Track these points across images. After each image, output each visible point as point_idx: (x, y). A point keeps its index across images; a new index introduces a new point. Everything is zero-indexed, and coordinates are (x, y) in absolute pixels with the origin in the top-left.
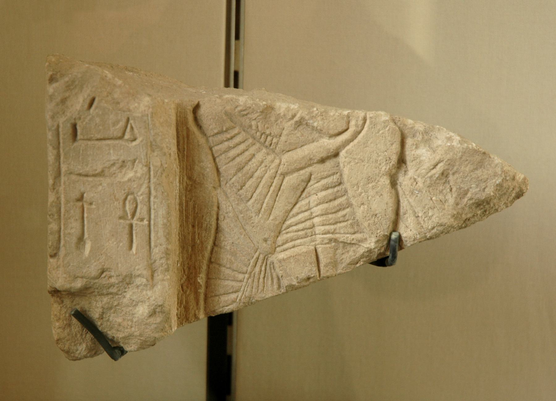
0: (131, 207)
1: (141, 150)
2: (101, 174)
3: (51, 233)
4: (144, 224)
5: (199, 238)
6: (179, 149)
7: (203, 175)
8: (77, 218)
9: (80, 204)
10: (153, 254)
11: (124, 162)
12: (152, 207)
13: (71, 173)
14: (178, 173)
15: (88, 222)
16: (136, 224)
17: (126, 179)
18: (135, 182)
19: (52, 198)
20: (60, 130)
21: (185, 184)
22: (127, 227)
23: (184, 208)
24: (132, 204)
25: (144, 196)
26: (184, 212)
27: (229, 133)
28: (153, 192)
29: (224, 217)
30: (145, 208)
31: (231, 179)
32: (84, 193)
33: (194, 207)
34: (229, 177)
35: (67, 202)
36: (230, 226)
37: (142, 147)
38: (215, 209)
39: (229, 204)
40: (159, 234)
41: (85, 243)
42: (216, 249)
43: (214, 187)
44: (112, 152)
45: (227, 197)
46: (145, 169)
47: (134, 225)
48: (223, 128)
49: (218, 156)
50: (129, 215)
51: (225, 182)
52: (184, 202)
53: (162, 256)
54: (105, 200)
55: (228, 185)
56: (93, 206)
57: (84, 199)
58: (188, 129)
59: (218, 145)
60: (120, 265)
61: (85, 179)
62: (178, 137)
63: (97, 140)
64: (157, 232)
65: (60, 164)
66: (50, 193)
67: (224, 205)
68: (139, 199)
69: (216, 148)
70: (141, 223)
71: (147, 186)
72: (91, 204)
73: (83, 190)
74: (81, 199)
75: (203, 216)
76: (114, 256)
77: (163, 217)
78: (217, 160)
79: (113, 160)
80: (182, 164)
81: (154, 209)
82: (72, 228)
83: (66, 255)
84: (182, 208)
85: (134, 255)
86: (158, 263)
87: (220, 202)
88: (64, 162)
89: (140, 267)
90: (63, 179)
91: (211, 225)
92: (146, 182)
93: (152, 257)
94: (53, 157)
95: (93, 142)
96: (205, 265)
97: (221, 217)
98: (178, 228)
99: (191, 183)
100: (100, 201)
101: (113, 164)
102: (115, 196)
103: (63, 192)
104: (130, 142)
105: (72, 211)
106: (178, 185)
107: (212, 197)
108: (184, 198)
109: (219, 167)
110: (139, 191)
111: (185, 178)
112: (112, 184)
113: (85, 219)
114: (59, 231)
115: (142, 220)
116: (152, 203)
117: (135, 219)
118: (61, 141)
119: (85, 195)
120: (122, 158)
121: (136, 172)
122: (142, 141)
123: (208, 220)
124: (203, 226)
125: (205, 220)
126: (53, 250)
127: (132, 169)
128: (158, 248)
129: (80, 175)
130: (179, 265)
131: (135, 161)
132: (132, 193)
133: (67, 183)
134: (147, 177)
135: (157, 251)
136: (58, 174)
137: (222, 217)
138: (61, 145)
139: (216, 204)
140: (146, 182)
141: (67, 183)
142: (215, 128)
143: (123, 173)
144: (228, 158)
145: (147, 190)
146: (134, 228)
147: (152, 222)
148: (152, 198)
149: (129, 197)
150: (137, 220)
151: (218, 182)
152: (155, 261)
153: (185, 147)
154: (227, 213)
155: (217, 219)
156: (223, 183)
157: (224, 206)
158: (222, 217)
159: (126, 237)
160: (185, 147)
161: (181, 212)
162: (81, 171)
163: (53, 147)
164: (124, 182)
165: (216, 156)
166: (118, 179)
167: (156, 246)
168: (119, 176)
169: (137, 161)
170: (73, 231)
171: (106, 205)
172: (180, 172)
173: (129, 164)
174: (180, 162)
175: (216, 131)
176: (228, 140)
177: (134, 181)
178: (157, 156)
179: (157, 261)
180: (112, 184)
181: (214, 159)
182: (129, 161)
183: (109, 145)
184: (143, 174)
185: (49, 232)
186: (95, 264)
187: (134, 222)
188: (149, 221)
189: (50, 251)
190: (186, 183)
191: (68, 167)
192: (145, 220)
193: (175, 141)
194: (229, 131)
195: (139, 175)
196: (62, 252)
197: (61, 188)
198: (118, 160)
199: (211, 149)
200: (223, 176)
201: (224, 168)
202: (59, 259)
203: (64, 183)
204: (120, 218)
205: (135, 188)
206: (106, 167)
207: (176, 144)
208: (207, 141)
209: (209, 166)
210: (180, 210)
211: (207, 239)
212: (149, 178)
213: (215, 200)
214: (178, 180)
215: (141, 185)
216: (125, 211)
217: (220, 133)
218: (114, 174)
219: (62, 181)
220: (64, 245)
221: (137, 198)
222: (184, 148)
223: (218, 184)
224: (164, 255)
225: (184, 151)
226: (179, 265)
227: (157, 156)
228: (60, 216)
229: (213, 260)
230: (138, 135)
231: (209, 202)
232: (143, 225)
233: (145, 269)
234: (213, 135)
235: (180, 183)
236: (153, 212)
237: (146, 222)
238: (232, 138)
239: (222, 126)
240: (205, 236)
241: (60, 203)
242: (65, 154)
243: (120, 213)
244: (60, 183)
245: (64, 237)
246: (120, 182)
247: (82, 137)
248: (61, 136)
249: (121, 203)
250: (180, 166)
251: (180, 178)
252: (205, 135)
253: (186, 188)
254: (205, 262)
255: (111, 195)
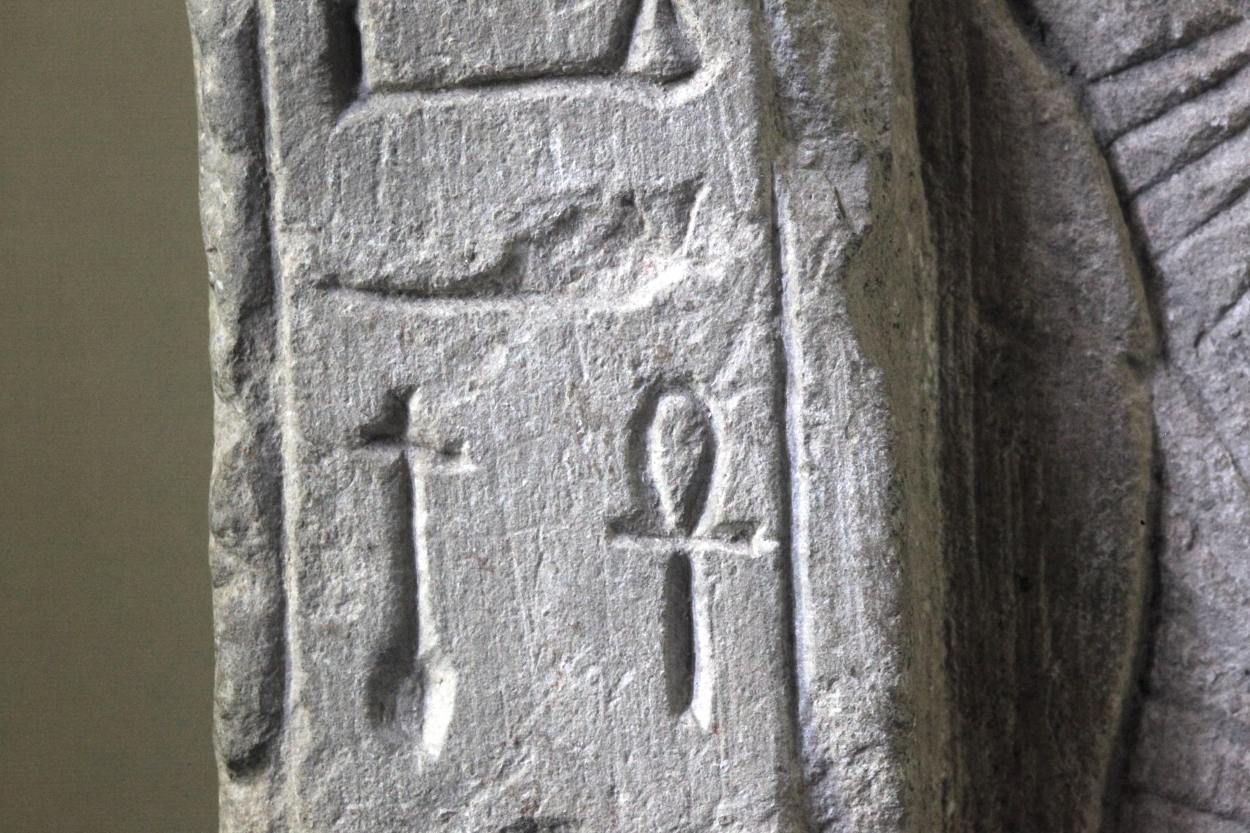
0: (679, 464)
1: (727, 130)
2: (503, 278)
3: (234, 635)
4: (755, 554)
5: (1057, 652)
6: (927, 150)
7: (1071, 290)
8: (373, 536)
9: (390, 456)
10: (807, 733)
11: (626, 200)
12: (799, 456)
13: (331, 283)
14: (932, 286)
15: (438, 553)
16: (708, 557)
17: (641, 300)
18: (699, 316)
19: (230, 428)
20: (267, 38)
21: (971, 347)
22: (659, 575)
23: (970, 481)
24: (684, 442)
25: (750, 391)
26: (972, 505)
27: (1204, 54)
28: (800, 368)
29: (1195, 531)
30: (759, 463)
31: (1224, 311)
32: (410, 391)
33: (1026, 478)
34: (1216, 301)
35: (316, 451)
36: (1228, 579)
37: (731, 110)
38: (1144, 481)
39: (1216, 451)
40: (844, 611)
41: (422, 681)
42: (1153, 712)
43: (1132, 361)
44: (557, 145)
45: (1208, 419)
46: (751, 237)
47: (698, 567)
48: (1166, 28)
49: (1141, 191)
50: (667, 505)
51: (1190, 331)
52: (969, 446)
53: (863, 737)
54: (530, 424)
55: (1208, 347)
56: (464, 466)
57: (413, 432)
58: (975, 34)
59: (1146, 121)
60: (623, 799)
61: (411, 309)
62: (922, 83)
63: (476, 83)
64: (831, 598)
65: (267, 235)
66: (221, 410)
67: (1191, 457)
68: (721, 412)
69: (1136, 139)
70: (740, 550)
71: (761, 332)
72: (449, 452)
73: (398, 374)
74: (389, 425)
75: (1077, 526)
76: (591, 749)
77: (861, 511)
78: (1144, 206)
79: (568, 193)
80: (948, 233)
81: (812, 468)
82: (345, 598)
83: (315, 759)
84: (960, 481)
85: (703, 739)
86: (843, 778)
87: (1166, 445)
88: (290, 220)
89: (740, 803)
90: (288, 317)
91: (1125, 574)
92: (757, 308)
93: (807, 747)
94: (228, 198)
95: (447, 100)
96: (1096, 802)
97: (1178, 531)
98: (941, 597)
99: (1002, 341)
100: (498, 434)
101: (567, 223)
102: (585, 399)
103: (289, 390)
104: (656, 89)
105: (345, 501)
106: (933, 350)
107: (1127, 417)
108: (968, 427)
109: (1156, 246)
110: (719, 365)
111: (972, 312)
112: (567, 333)
113: (421, 544)
114: (276, 619)
115: (740, 530)
116: (796, 433)
117: (702, 527)
118: (272, 102)
119: (415, 404)
120: (617, 181)
121: (699, 257)
122: (724, 77)
123: (1107, 547)
124: (1082, 579)
125: (1091, 548)
126: (246, 732)
127: (677, 241)
128: (837, 695)
129: (381, 288)
130: (952, 806)
131: (685, 194)
132: (682, 383)
133: (312, 342)
134: (764, 281)
135: (835, 711)
136: (258, 301)
137: (1183, 527)
138: (274, 122)
139: (1148, 455)
140: (757, 308)
141: (312, 342)
142: (1125, 29)
143: (625, 268)
144: (1205, 192)
145: (766, 355)
146: (699, 581)
147: (801, 544)
148: (796, 406)
149: (667, 405)
150: (715, 536)
151: (1149, 329)
152: (825, 767)
153: (967, 136)
154: (1208, 505)
155: (1156, 542)
156: (1180, 339)
157: (1194, 468)
158: (1183, 527)
159: (652, 633)
160: (967, 136)
161: (953, 500)
162: (389, 268)
163: (228, 138)
164: (630, 320)
165: (1133, 184)
166: (596, 304)
167: (828, 682)
168: (602, 288)
169: (701, 196)
170: (354, 612)
171: (535, 456)
172: (942, 278)
173: (656, 215)
174: (937, 224)
175: (1129, 45)
176: (1200, 90)
177: (689, 307)
178: (813, 165)
179: (840, 769)
180: (567, 333)
181: (1126, 202)
182: (657, 193)
183: (539, 110)
184: (739, 266)
185: (220, 627)
186: (483, 797)
187: (699, 546)
188: (784, 535)
189: (226, 737)
190: (978, 337)
191: (314, 249)
192: (761, 531)
193: (907, 103)
194: (1202, 45)
195: (715, 271)
196: (298, 737)
197: (283, 372)
198: (593, 191)
199: (1105, 146)
200: (1178, 301)
201: (1184, 247)
202: (278, 780)
203: (297, 343)
204: (616, 527)
205: (694, 349)
206: (526, 239)
207: (913, 121)
208: (1084, 105)
209: (1101, 238)
210: (945, 493)
211: (1104, 652)
212: (776, 290)
213: (1140, 434)
214: (929, 323)
215: (732, 329)
216: (640, 486)
217: (1155, 51)
218: (575, 274)
219: (285, 328)
220: (305, 699)
221: (712, 404)
222: (959, 145)
223: (1151, 344)
224: (875, 731)
225: (960, 159)
226: (952, 806)
227: (813, 165)
228: (275, 531)
229: (1142, 776)
230: (702, 47)
231: (1108, 443)
232: (749, 562)
233: (768, 816)
234: (1116, 71)
235: (942, 343)
236: (801, 482)
237: (762, 545)
238: (1220, 80)
239: (1166, 18)
240: (1091, 640)
241: (276, 460)
242: (298, 175)
243: (613, 498)
244: (273, 344)
245: (306, 652)
246: (611, 321)
247: (387, 74)
248: (272, 73)
249: (620, 441)
250: (940, 245)
251: (941, 313)
252: (1073, 70)
253: (980, 371)
254: (1096, 787)
255: (559, 397)
